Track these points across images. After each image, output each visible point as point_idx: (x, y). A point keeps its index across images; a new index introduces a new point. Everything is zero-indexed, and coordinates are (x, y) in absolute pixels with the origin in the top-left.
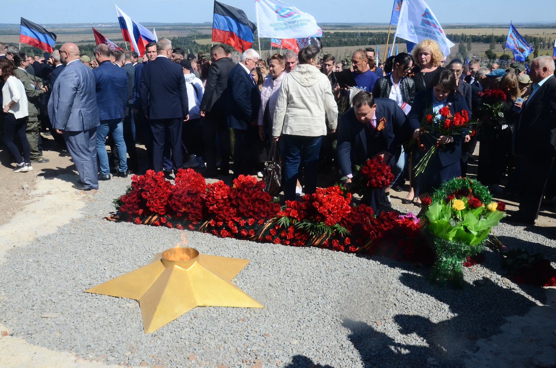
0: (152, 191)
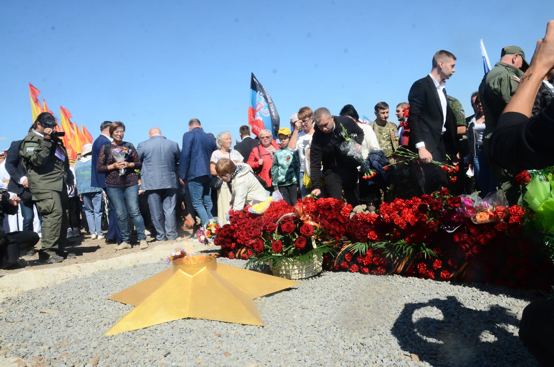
0: (240, 222)
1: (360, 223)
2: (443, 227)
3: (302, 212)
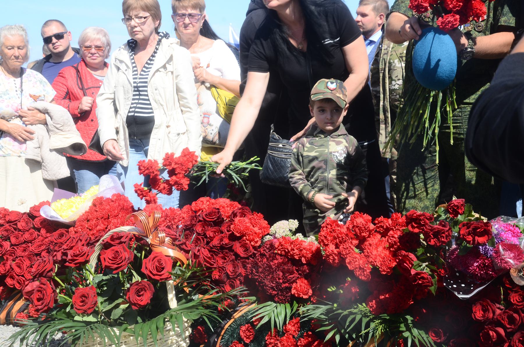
1: (277, 259)
2: (449, 284)
3: (151, 224)
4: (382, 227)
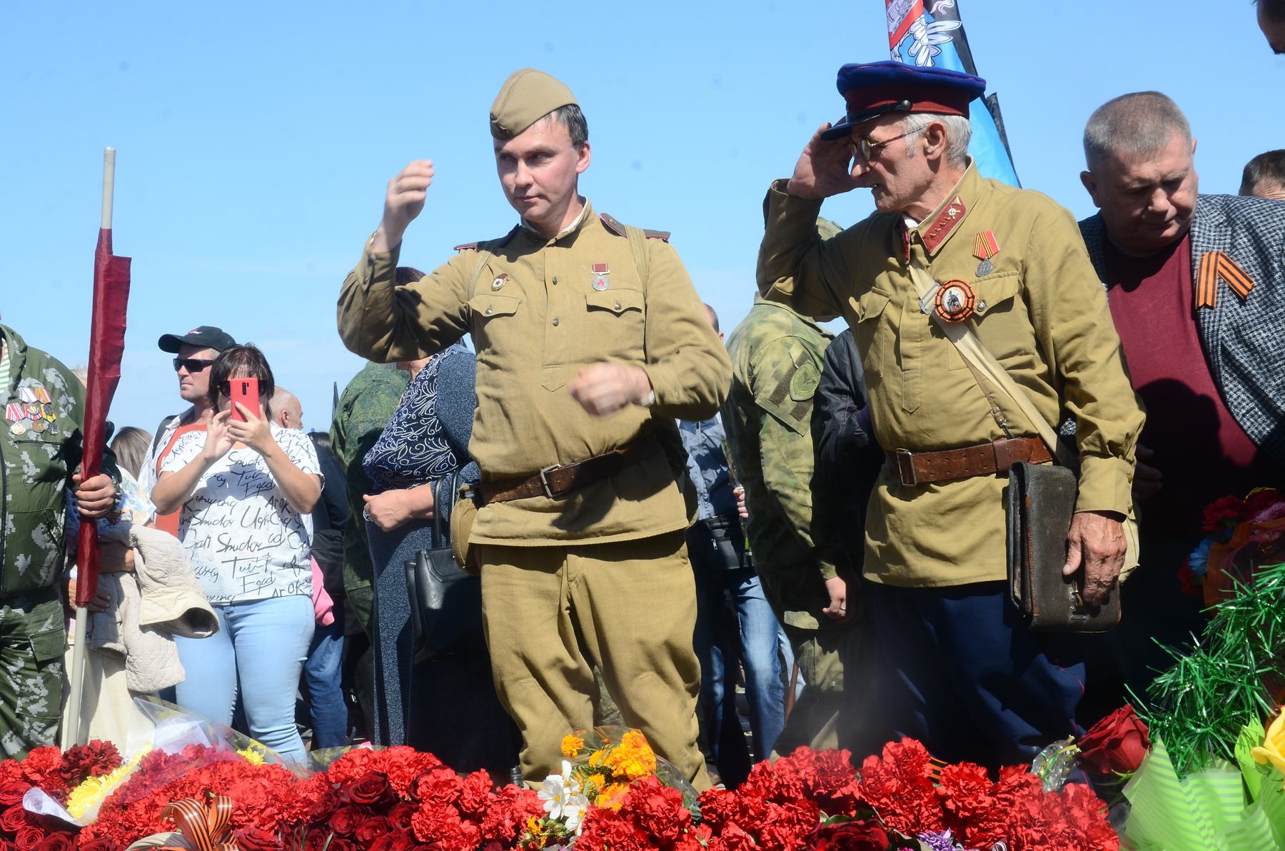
4: (715, 811)
